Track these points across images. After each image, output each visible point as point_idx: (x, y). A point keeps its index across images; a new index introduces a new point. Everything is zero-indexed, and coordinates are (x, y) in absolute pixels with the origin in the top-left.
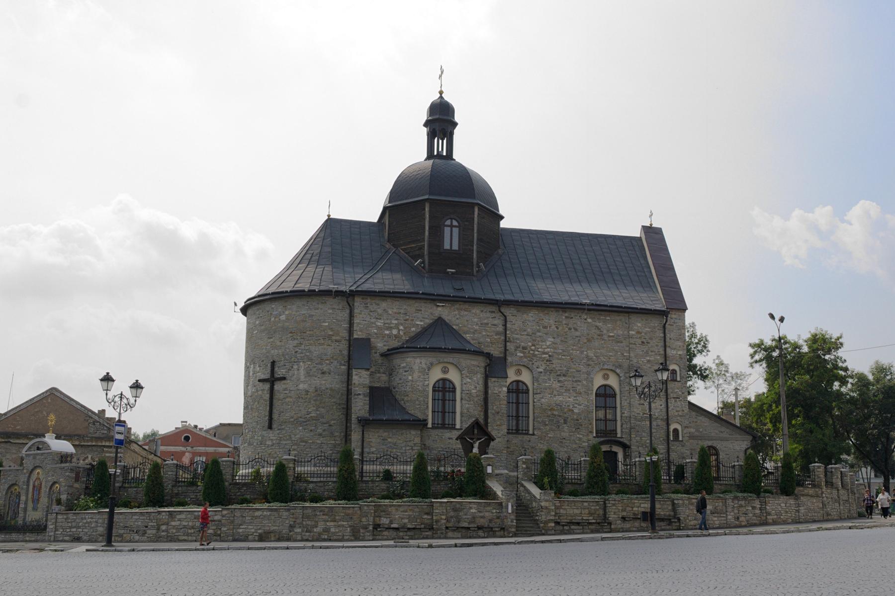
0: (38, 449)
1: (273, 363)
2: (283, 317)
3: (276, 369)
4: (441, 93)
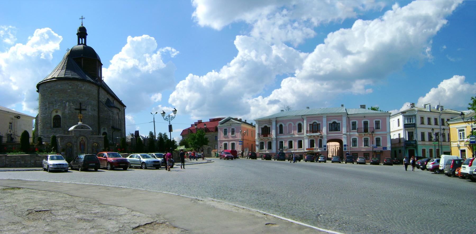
0: (82, 128)
1: (80, 104)
2: (83, 88)
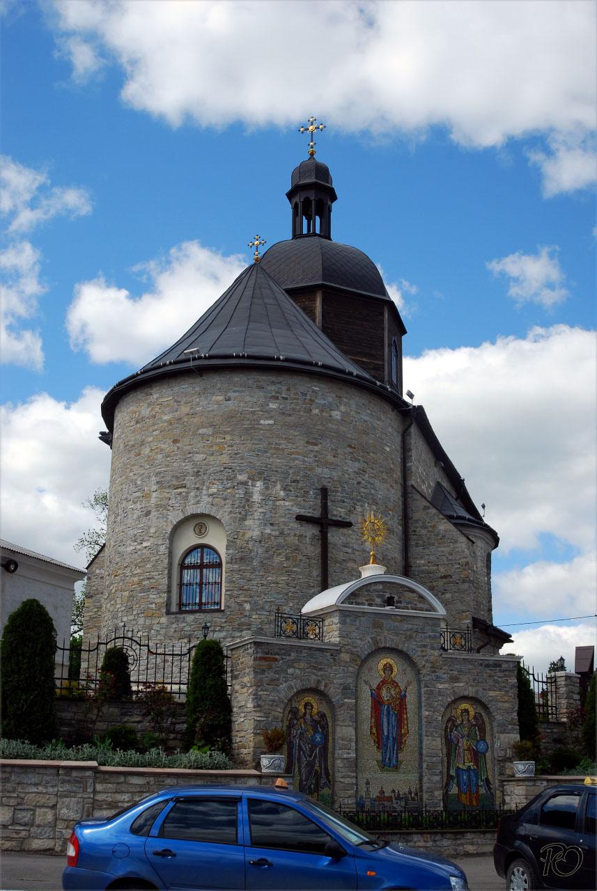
0: (390, 602)
1: (324, 492)
2: (336, 414)
3: (329, 504)
4: (312, 154)
